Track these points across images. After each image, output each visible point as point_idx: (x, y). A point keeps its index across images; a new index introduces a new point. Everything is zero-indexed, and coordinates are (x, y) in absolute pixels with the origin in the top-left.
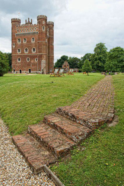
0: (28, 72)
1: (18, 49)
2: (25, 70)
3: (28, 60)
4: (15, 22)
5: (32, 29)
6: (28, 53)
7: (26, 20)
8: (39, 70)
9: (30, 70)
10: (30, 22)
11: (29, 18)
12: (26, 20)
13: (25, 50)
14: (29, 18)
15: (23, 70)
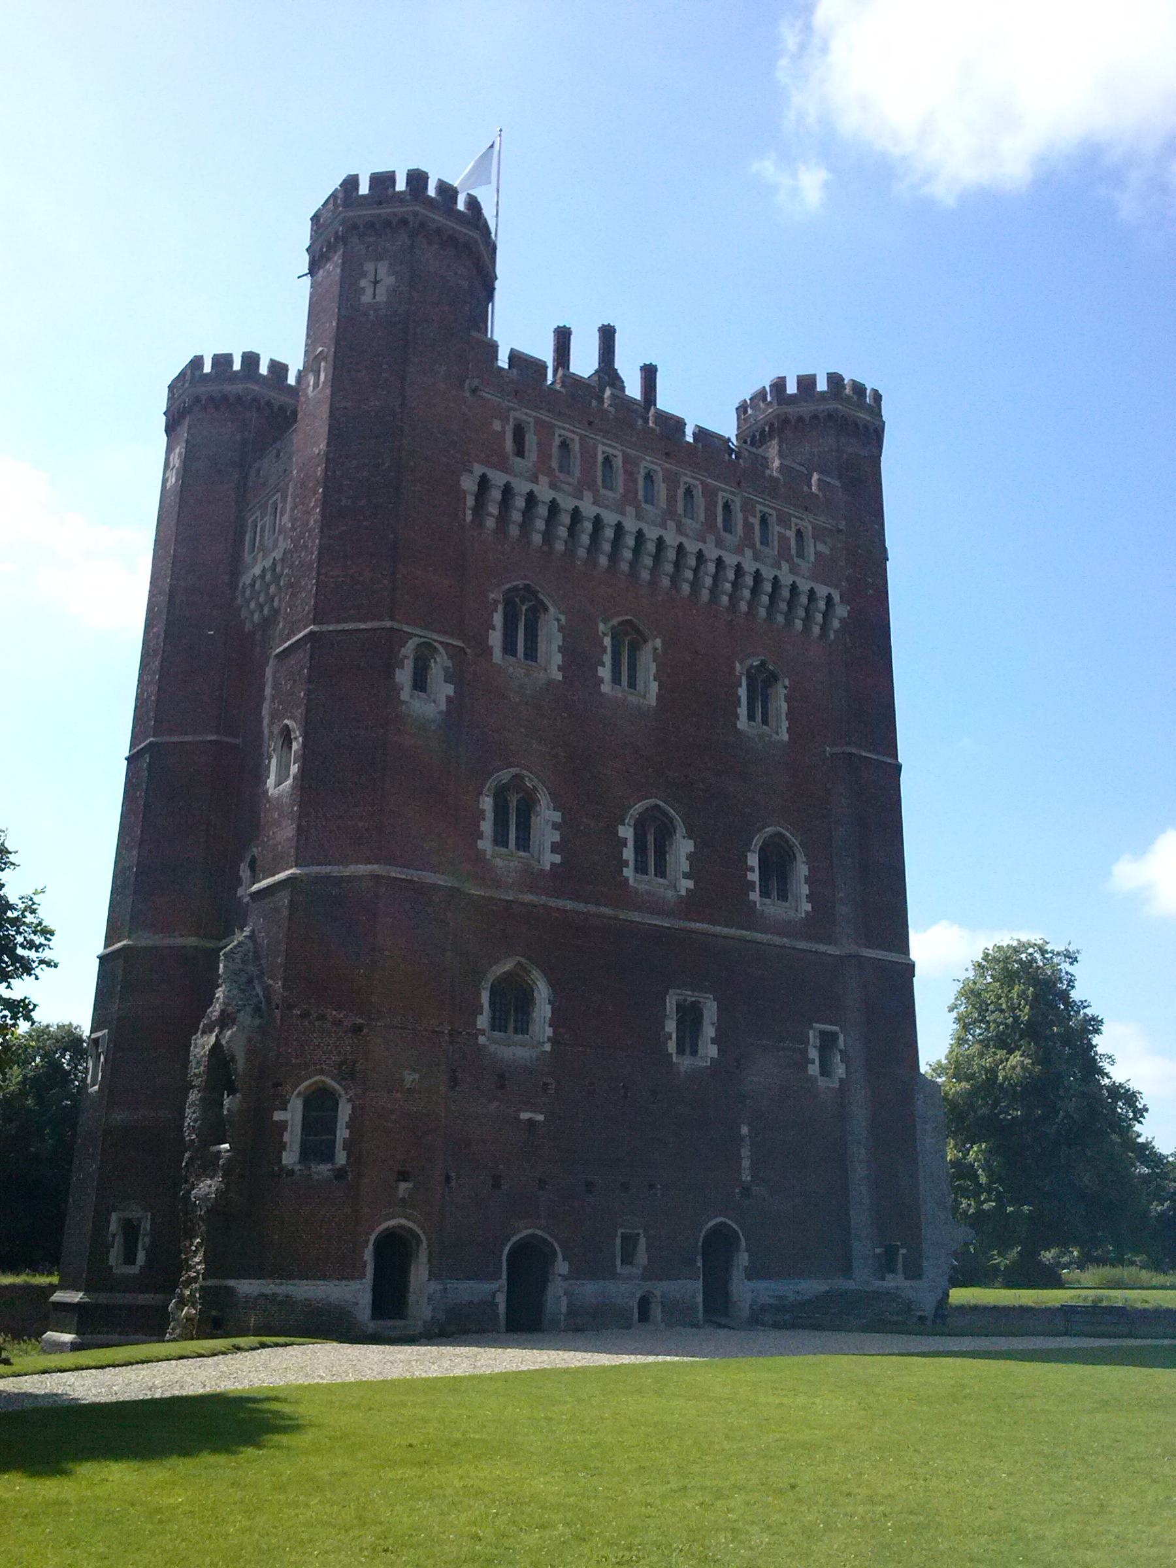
0: (692, 1289)
1: (505, 776)
2: (629, 1242)
3: (690, 1018)
4: (405, 255)
5: (755, 521)
6: (691, 906)
7: (563, 337)
8: (887, 1264)
9: (719, 1246)
10: (634, 389)
11: (607, 335)
12: (563, 337)
13: (626, 832)
14: (607, 335)
15: (592, 1265)
